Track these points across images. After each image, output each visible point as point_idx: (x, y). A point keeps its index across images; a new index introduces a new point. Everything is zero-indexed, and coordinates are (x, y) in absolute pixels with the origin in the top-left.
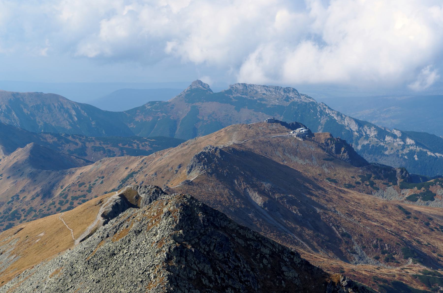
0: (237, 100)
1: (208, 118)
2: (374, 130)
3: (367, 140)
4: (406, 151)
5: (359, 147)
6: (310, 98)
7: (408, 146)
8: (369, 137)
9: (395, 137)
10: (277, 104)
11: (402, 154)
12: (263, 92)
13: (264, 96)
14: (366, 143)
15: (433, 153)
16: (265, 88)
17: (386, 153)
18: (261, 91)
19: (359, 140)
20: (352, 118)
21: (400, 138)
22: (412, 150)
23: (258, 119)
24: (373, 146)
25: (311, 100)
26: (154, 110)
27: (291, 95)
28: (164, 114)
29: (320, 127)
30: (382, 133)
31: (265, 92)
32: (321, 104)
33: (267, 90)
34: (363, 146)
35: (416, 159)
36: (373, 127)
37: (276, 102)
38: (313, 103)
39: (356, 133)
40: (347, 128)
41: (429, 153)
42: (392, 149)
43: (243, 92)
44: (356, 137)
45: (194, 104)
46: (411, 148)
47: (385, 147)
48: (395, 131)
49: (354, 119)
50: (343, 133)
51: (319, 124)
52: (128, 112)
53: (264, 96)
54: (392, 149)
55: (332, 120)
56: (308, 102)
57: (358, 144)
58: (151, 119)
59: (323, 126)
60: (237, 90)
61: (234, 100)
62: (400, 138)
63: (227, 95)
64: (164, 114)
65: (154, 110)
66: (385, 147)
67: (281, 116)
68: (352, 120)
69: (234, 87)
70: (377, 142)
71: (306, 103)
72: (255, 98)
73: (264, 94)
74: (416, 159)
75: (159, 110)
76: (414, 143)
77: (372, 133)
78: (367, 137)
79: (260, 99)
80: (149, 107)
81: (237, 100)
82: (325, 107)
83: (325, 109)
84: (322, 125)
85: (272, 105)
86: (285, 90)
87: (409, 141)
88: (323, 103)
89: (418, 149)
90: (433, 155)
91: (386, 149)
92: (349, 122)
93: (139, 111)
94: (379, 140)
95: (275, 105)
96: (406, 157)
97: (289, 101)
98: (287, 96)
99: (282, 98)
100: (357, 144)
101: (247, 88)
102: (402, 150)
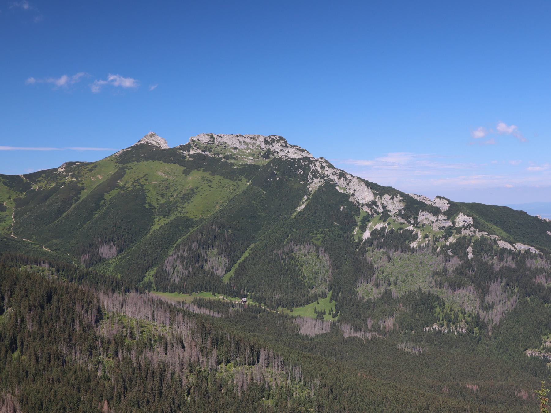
0: (192, 159)
1: (132, 185)
3: (385, 221)
5: (367, 235)
6: (303, 151)
8: (389, 216)
9: (436, 211)
10: (250, 162)
11: (444, 247)
12: (235, 146)
14: (379, 226)
15: (511, 243)
17: (414, 244)
19: (369, 221)
20: (362, 180)
21: (444, 213)
22: (465, 237)
23: (210, 186)
24: (392, 231)
25: (305, 155)
27: (276, 147)
28: (74, 179)
30: (413, 206)
32: (320, 160)
33: (240, 142)
34: (374, 233)
35: (470, 256)
36: (399, 196)
37: (249, 160)
38: (307, 159)
39: (366, 209)
40: (351, 199)
42: (426, 236)
43: (206, 147)
44: (365, 215)
46: (464, 232)
48: (438, 200)
49: (364, 181)
50: (342, 208)
53: (235, 152)
54: (426, 236)
55: (329, 186)
56: (297, 156)
58: (53, 185)
60: (197, 144)
64: (74, 179)
65: (64, 173)
67: (248, 182)
68: (362, 183)
70: (401, 224)
71: (294, 159)
72: (221, 156)
73: (236, 148)
76: (472, 223)
77: (394, 206)
78: (385, 216)
79: (227, 157)
81: (192, 159)
82: (325, 164)
85: (241, 165)
86: (269, 139)
87: (462, 219)
88: (322, 158)
91: (415, 237)
93: (44, 175)
95: (247, 164)
98: (269, 149)
99: (260, 153)
100: (363, 229)
101: (213, 141)
102: (446, 237)
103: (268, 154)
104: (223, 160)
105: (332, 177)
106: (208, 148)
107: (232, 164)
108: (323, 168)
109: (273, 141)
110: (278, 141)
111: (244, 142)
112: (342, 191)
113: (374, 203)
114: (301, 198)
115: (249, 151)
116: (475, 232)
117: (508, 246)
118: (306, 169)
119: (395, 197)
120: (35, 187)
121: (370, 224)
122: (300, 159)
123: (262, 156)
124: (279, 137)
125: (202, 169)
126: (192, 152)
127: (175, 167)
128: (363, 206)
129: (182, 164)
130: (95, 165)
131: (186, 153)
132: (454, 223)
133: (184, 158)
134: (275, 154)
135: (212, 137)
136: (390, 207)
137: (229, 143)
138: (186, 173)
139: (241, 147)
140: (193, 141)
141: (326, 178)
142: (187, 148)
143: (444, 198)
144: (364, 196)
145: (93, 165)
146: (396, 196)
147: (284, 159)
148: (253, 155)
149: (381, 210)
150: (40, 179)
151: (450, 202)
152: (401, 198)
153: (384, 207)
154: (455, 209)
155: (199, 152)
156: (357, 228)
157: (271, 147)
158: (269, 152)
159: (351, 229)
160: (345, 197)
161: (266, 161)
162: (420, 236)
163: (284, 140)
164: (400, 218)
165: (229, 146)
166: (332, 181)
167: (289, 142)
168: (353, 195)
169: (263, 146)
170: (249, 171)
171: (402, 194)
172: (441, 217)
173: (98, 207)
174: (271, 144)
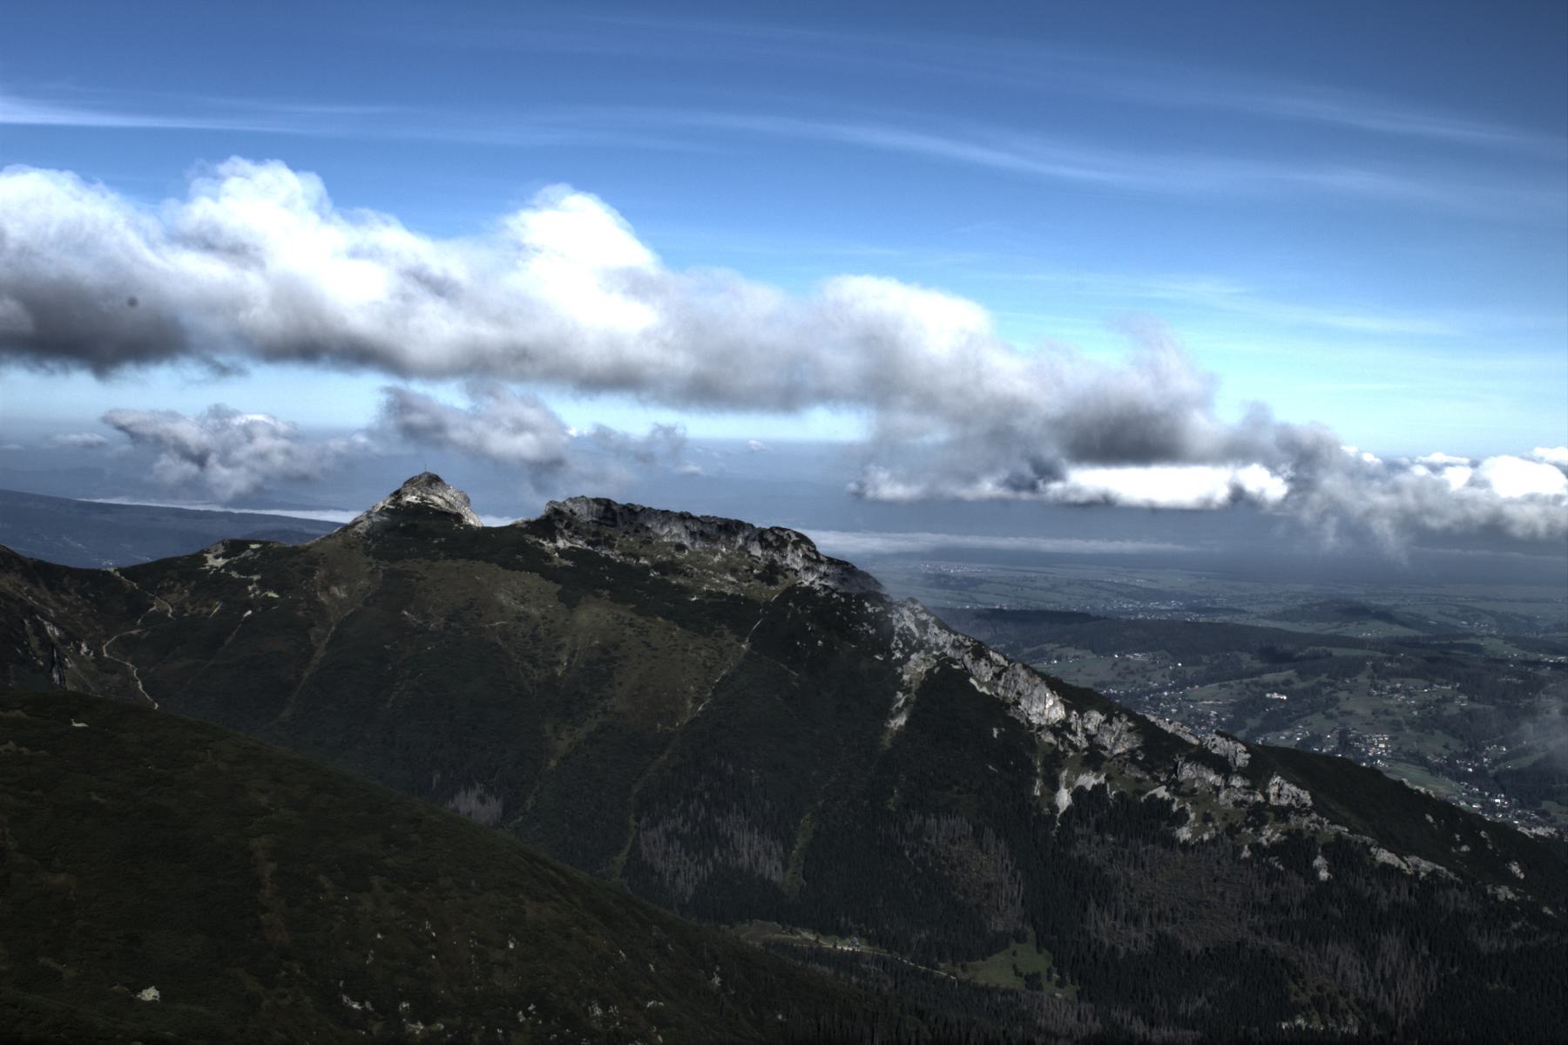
0: (569, 563)
2: (1130, 730)
4: (1270, 835)
5: (1064, 798)
7: (1282, 813)
9: (1222, 765)
10: (729, 591)
12: (677, 540)
13: (680, 556)
14: (1088, 781)
16: (688, 523)
17: (1184, 834)
21: (1243, 772)
22: (1299, 832)
23: (648, 645)
26: (234, 574)
34: (1078, 794)
37: (727, 584)
39: (1049, 738)
40: (1011, 713)
43: (596, 534)
45: (398, 566)
47: (1175, 808)
51: (898, 684)
52: (132, 572)
53: (680, 556)
57: (1056, 788)
59: (913, 697)
63: (533, 539)
65: (234, 574)
66: (1175, 808)
67: (743, 641)
69: (566, 510)
70: (1138, 780)
72: (643, 561)
73: (681, 547)
75: (255, 578)
80: (221, 562)
81: (569, 563)
82: (924, 617)
84: (907, 691)
85: (709, 593)
87: (1282, 791)
89: (1331, 830)
91: (1181, 818)
97: (775, 582)
98: (773, 562)
99: (752, 569)
100: (1053, 786)
103: (772, 572)
107: (682, 590)
110: (796, 545)
120: (163, 606)
121: (1064, 774)
123: (757, 577)
125: (606, 593)
127: (532, 580)
131: (548, 545)
133: (548, 557)
138: (569, 600)
146: (1118, 716)
148: (734, 572)
149: (1080, 740)
153: (1090, 737)
161: (773, 592)
162: (1192, 816)
166: (953, 661)
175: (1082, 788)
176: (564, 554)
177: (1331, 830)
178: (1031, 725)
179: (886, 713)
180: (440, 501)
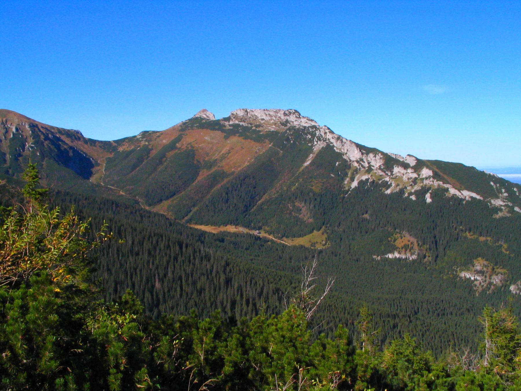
1: (186, 147)
5: (355, 184)
6: (312, 120)
8: (372, 170)
9: (406, 166)
10: (273, 129)
12: (262, 118)
13: (262, 122)
14: (364, 178)
15: (459, 190)
16: (266, 112)
17: (388, 192)
18: (261, 116)
19: (357, 173)
21: (412, 168)
25: (313, 124)
27: (292, 118)
29: (311, 155)
30: (390, 162)
31: (264, 117)
32: (324, 127)
33: (266, 115)
35: (429, 200)
36: (380, 154)
37: (273, 128)
39: (356, 164)
40: (345, 157)
41: (453, 191)
42: (398, 185)
44: (354, 169)
46: (426, 182)
49: (355, 143)
50: (337, 163)
52: (115, 141)
53: (262, 122)
55: (329, 148)
56: (307, 125)
58: (133, 147)
59: (315, 155)
60: (236, 117)
61: (228, 127)
62: (412, 168)
64: (147, 143)
67: (270, 144)
71: (305, 127)
73: (263, 119)
74: (429, 200)
77: (377, 162)
78: (369, 170)
79: (257, 126)
81: (231, 128)
83: (325, 133)
85: (266, 131)
86: (287, 112)
88: (325, 126)
89: (436, 183)
90: (457, 193)
92: (349, 147)
94: (385, 172)
95: (270, 131)
96: (413, 198)
100: (352, 179)
101: (247, 114)
104: (254, 128)
105: (332, 140)
106: (242, 120)
107: (260, 131)
108: (325, 133)
109: (290, 113)
110: (294, 113)
111: (269, 114)
112: (338, 151)
113: (362, 160)
114: (307, 156)
115: (272, 121)
116: (433, 182)
117: (457, 193)
118: (313, 135)
119: (377, 155)
120: (121, 149)
122: (309, 127)
124: (295, 110)
126: (231, 123)
127: (218, 133)
128: (353, 161)
129: (223, 131)
130: (162, 133)
131: (227, 123)
132: (419, 175)
133: (225, 126)
134: (291, 123)
135: (246, 111)
136: (373, 163)
137: (259, 116)
138: (226, 138)
139: (267, 118)
140: (233, 114)
141: (327, 141)
142: (228, 119)
143: (413, 156)
144: (354, 155)
145: (160, 133)
147: (297, 127)
149: (366, 165)
150: (125, 143)
151: (417, 159)
152: (381, 156)
153: (369, 163)
154: (420, 164)
155: (237, 122)
156: (348, 179)
157: (288, 118)
158: (287, 121)
159: (343, 179)
160: (339, 156)
162: (393, 185)
163: (298, 112)
164: (380, 171)
165: (258, 117)
166: (332, 143)
167: (302, 114)
168: (346, 153)
169: (283, 117)
170: (272, 136)
171: (382, 153)
172: (409, 170)
173: (161, 163)
174: (289, 116)
175: (362, 180)
176: (230, 125)
177: (436, 183)
178: (350, 160)
179: (304, 161)
180: (204, 116)
